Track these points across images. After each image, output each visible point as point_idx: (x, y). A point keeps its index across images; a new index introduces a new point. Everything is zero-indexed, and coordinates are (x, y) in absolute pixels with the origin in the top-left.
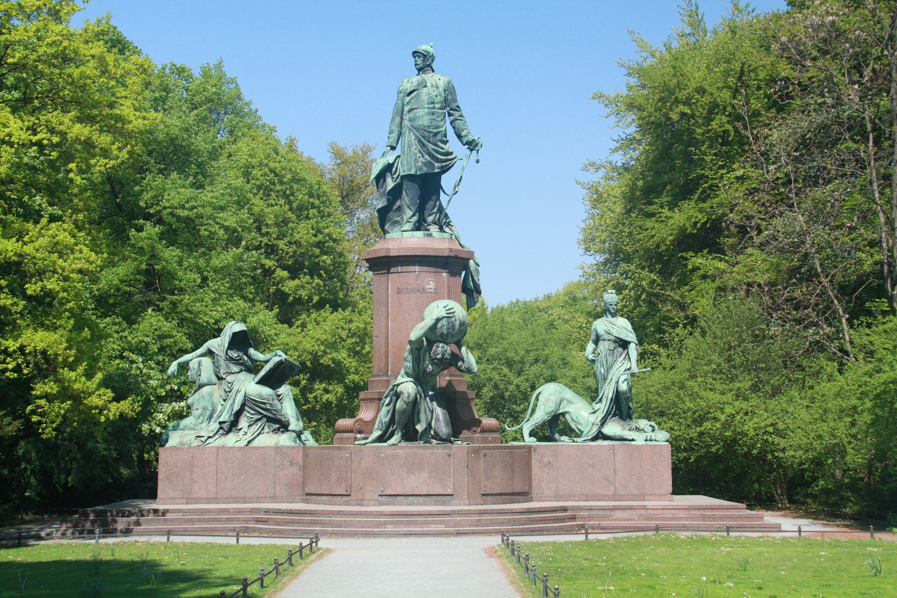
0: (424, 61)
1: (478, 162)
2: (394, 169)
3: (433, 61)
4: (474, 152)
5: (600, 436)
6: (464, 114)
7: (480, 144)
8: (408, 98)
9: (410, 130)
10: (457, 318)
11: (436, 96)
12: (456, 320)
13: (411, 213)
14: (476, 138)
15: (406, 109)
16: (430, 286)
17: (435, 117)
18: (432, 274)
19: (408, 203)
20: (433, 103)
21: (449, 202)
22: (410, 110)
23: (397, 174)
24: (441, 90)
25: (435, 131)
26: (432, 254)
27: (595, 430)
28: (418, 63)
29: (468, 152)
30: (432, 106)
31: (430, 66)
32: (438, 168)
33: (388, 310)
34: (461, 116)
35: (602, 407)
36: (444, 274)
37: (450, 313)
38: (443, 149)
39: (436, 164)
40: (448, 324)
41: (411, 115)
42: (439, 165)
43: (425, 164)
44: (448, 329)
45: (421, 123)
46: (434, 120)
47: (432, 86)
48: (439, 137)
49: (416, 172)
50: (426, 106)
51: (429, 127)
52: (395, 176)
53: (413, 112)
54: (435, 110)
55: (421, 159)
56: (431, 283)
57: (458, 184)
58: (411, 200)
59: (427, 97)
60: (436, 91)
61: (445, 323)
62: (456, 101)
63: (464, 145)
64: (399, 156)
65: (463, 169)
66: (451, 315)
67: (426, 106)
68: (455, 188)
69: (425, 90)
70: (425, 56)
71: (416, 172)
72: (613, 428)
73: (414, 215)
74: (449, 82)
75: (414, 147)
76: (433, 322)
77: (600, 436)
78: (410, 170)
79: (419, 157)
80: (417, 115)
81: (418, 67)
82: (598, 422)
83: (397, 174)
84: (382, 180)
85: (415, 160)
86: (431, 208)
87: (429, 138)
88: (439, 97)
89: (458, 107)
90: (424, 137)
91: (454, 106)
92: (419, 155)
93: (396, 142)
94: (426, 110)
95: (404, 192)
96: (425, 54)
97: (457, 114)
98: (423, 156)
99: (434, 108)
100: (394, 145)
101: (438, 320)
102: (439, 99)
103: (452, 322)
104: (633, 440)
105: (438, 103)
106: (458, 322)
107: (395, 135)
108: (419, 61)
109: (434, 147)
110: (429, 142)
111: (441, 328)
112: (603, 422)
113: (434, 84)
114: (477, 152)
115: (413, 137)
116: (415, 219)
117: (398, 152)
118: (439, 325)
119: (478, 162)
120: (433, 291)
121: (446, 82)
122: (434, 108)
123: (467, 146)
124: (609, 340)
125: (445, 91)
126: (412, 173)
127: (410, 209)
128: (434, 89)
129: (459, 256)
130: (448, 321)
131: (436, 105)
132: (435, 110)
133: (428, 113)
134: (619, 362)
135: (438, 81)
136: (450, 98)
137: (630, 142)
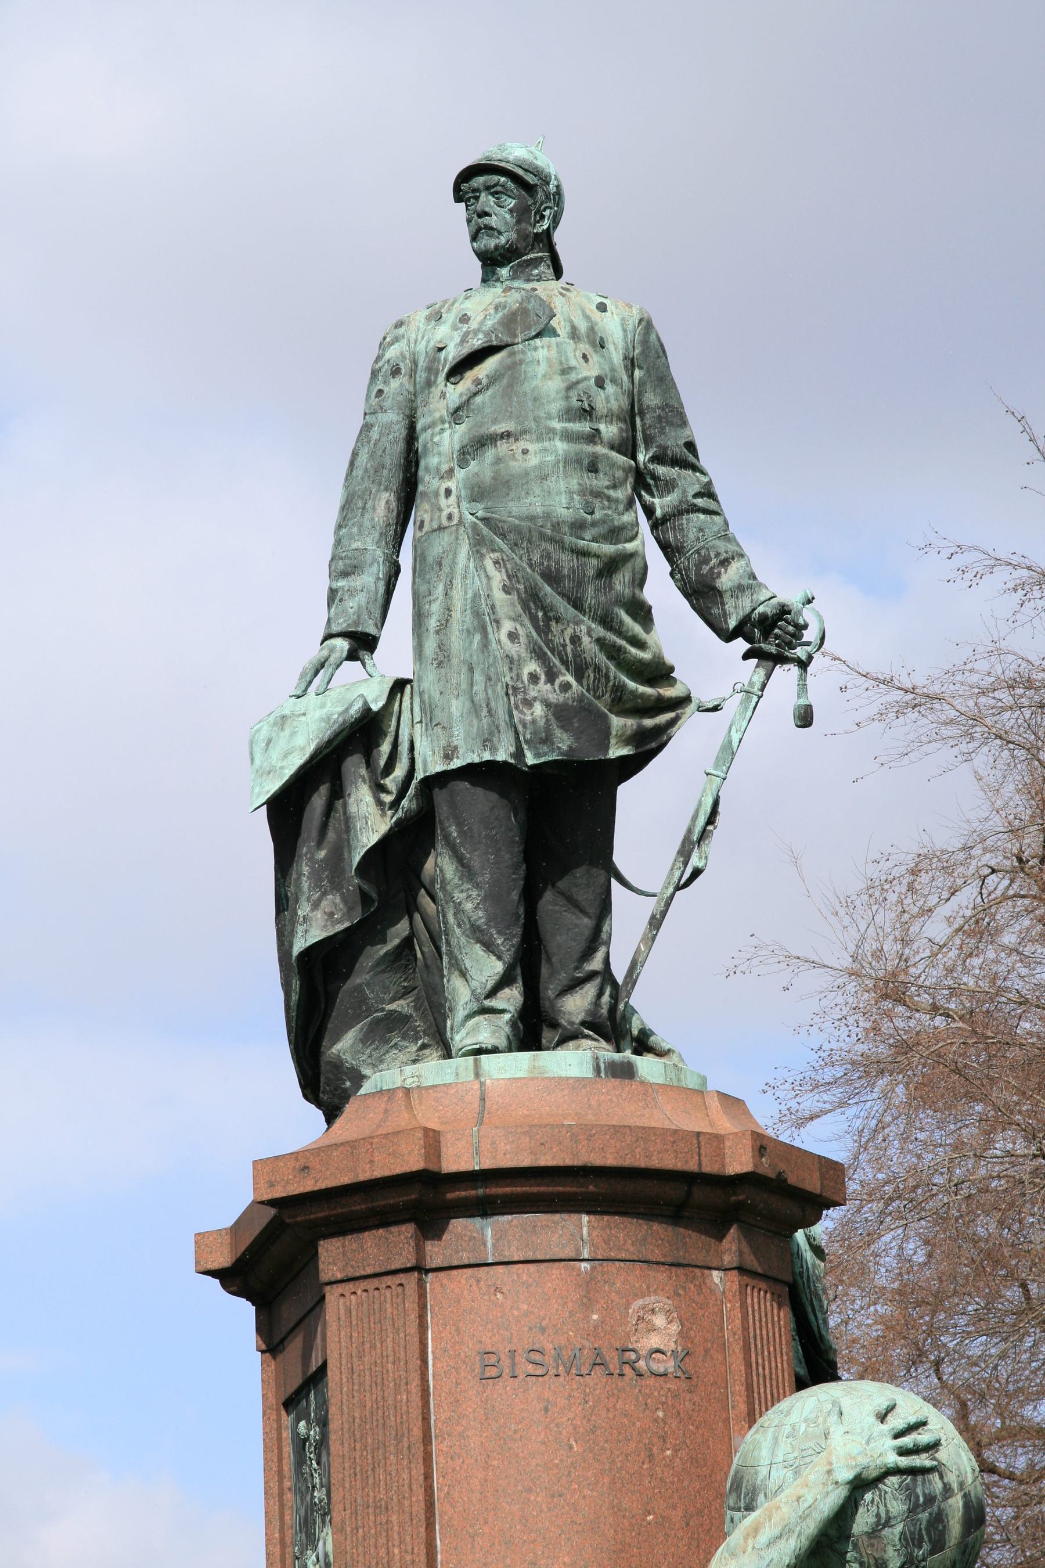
0: (521, 213)
1: (805, 718)
3: (556, 221)
4: (785, 675)
6: (718, 489)
7: (809, 635)
8: (456, 392)
9: (479, 544)
10: (952, 1479)
11: (600, 383)
12: (947, 1490)
13: (497, 967)
14: (791, 597)
16: (654, 1341)
17: (601, 482)
18: (661, 1275)
19: (480, 917)
20: (587, 413)
21: (656, 923)
22: (480, 443)
23: (400, 771)
24: (617, 358)
25: (608, 549)
26: (669, 1162)
28: (493, 221)
29: (750, 671)
30: (583, 427)
31: (546, 240)
32: (628, 741)
33: (428, 1477)
34: (708, 492)
37: (916, 1450)
38: (641, 645)
39: (617, 722)
40: (913, 1510)
41: (482, 466)
42: (630, 723)
43: (561, 713)
44: (910, 1540)
45: (538, 509)
46: (598, 494)
47: (574, 334)
48: (621, 582)
49: (519, 754)
50: (557, 425)
51: (578, 526)
52: (391, 782)
53: (490, 454)
54: (600, 449)
55: (543, 687)
56: (659, 1321)
57: (704, 835)
58: (492, 898)
59: (555, 385)
60: (594, 358)
61: (897, 1507)
62: (684, 423)
63: (728, 636)
64: (399, 686)
65: (728, 752)
66: (922, 1461)
67: (557, 425)
68: (685, 853)
69: (543, 351)
70: (529, 188)
71: (519, 754)
73: (504, 981)
74: (647, 325)
75: (507, 626)
76: (833, 1499)
78: (487, 742)
79: (534, 678)
80: (516, 466)
81: (489, 243)
83: (400, 771)
84: (318, 801)
85: (511, 691)
86: (578, 947)
87: (580, 584)
88: (610, 388)
89: (691, 446)
90: (552, 578)
91: (673, 441)
92: (533, 666)
93: (377, 612)
94: (561, 446)
96: (530, 179)
97: (689, 483)
98: (551, 677)
99: (594, 437)
100: (372, 630)
101: (860, 1485)
102: (609, 400)
103: (930, 1500)
105: (610, 417)
106: (956, 1503)
107: (370, 579)
109: (600, 631)
110: (577, 604)
111: (874, 1533)
113: (582, 326)
114: (803, 665)
115: (498, 578)
116: (511, 999)
118: (862, 1522)
119: (805, 718)
120: (670, 1366)
121: (632, 323)
122: (594, 437)
123: (741, 645)
125: (631, 364)
127: (489, 947)
128: (585, 347)
129: (792, 1180)
130: (910, 1493)
131: (602, 427)
132: (600, 449)
133: (573, 462)
135: (596, 316)
136: (652, 399)
137: (562, 1007)
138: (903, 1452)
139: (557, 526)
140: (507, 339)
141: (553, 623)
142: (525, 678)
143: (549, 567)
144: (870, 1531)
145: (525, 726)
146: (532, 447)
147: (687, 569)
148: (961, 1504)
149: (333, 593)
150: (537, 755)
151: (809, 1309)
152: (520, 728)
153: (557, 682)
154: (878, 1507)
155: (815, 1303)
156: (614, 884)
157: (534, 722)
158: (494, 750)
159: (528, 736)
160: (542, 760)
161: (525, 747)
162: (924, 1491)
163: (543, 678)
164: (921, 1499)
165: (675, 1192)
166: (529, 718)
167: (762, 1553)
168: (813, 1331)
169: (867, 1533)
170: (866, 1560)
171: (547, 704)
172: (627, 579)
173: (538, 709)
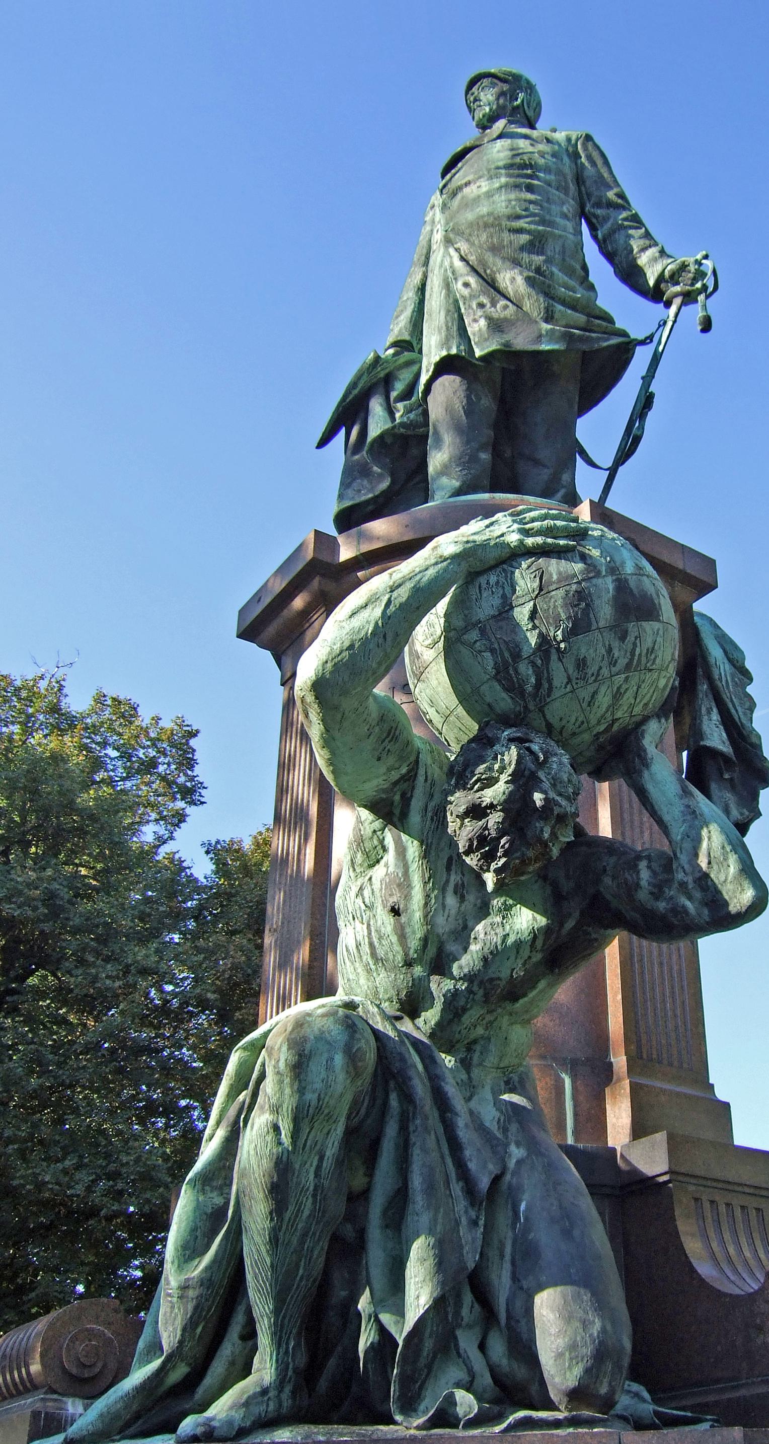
53: (459, 196)
71: (471, 351)
126: (454, 351)
139: (498, 218)
140: (478, 143)
141: (498, 275)
142: (474, 306)
143: (492, 242)
144: (497, 613)
145: (474, 335)
146: (483, 184)
147: (621, 263)
148: (611, 587)
150: (481, 350)
151: (730, 706)
152: (471, 337)
153: (498, 306)
154: (503, 588)
155: (735, 700)
156: (579, 461)
157: (480, 330)
158: (449, 349)
159: (477, 340)
160: (486, 351)
161: (474, 347)
162: (558, 569)
163: (489, 305)
164: (555, 577)
166: (477, 329)
167: (344, 624)
168: (736, 723)
169: (494, 617)
170: (496, 646)
171: (489, 319)
172: (557, 250)
173: (483, 323)
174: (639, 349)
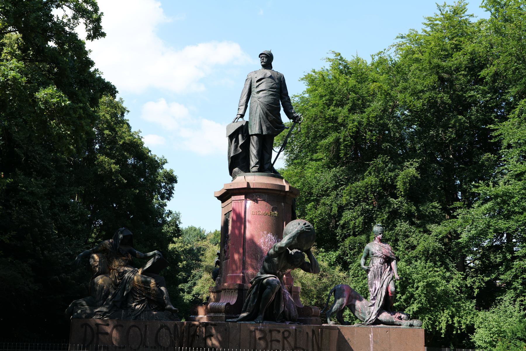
2: (244, 130)
5: (377, 322)
15: (254, 90)
27: (373, 317)
35: (379, 302)
36: (283, 204)
72: (385, 316)
77: (377, 322)
82: (375, 312)
95: (251, 147)
104: (400, 325)
108: (265, 60)
112: (379, 312)
117: (246, 118)
124: (380, 257)
134: (387, 272)
138: (306, 229)
149: (239, 109)
165: (279, 193)
174: (285, 130)
